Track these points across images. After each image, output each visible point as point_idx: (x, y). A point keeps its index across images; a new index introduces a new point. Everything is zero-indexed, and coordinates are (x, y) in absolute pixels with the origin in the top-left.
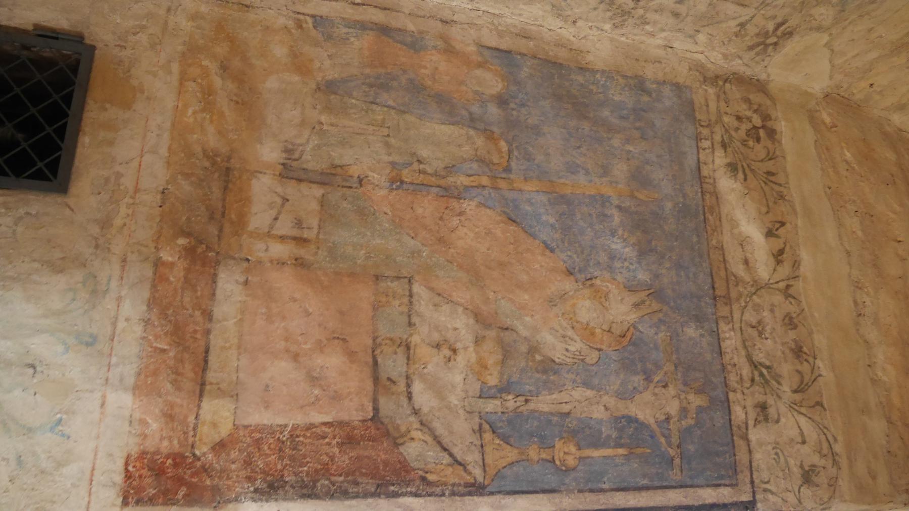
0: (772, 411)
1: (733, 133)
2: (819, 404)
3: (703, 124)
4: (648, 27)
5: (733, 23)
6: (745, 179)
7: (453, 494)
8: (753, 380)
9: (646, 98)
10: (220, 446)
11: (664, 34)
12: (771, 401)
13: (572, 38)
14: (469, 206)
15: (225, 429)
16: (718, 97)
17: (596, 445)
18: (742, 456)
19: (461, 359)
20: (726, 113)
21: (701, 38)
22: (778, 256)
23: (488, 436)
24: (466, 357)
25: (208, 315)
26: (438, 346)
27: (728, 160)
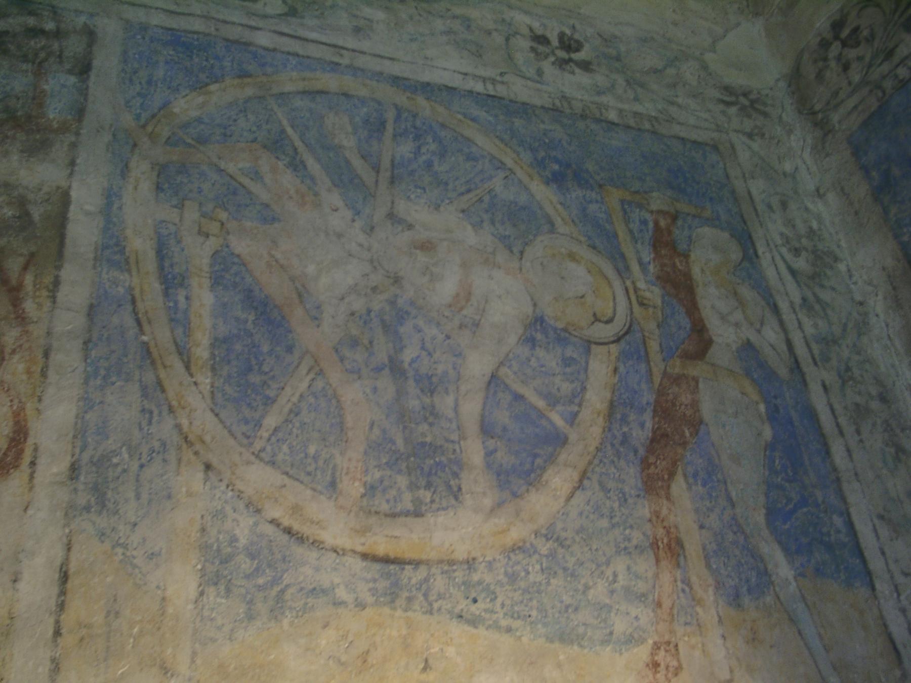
1: (867, 59)
3: (880, 94)
4: (815, 225)
5: (755, 146)
9: (896, 172)
11: (810, 206)
13: (880, 297)
16: (837, 106)
20: (850, 83)
21: (788, 167)
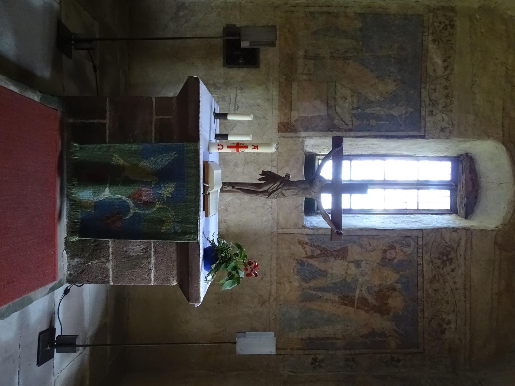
0: (434, 113)
2: (452, 111)
6: (438, 44)
7: (345, 131)
8: (429, 104)
10: (296, 121)
12: (434, 110)
14: (351, 62)
15: (296, 117)
16: (433, 16)
17: (381, 120)
18: (423, 124)
19: (347, 101)
22: (446, 68)
23: (354, 118)
24: (349, 100)
25: (291, 93)
26: (342, 98)
27: (434, 38)
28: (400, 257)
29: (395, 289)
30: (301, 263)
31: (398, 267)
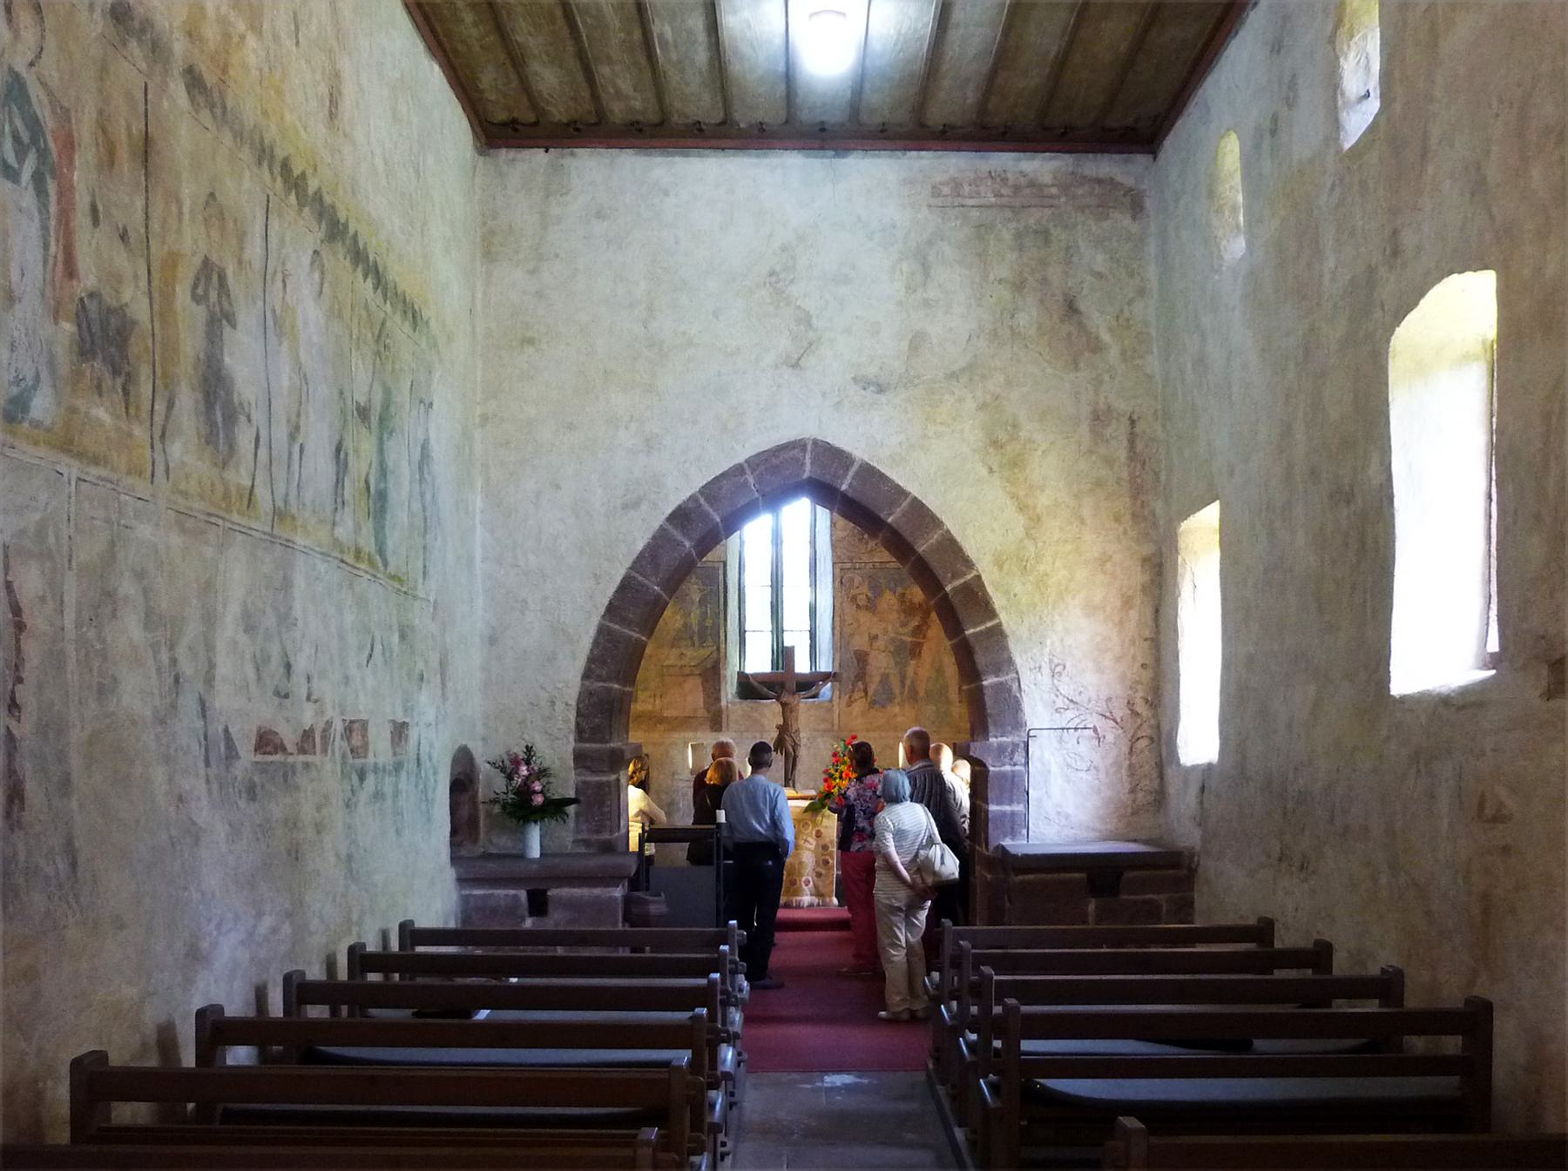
28: (865, 589)
29: (903, 595)
30: (873, 704)
31: (877, 591)
